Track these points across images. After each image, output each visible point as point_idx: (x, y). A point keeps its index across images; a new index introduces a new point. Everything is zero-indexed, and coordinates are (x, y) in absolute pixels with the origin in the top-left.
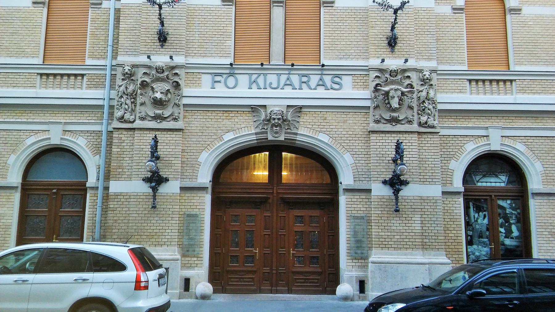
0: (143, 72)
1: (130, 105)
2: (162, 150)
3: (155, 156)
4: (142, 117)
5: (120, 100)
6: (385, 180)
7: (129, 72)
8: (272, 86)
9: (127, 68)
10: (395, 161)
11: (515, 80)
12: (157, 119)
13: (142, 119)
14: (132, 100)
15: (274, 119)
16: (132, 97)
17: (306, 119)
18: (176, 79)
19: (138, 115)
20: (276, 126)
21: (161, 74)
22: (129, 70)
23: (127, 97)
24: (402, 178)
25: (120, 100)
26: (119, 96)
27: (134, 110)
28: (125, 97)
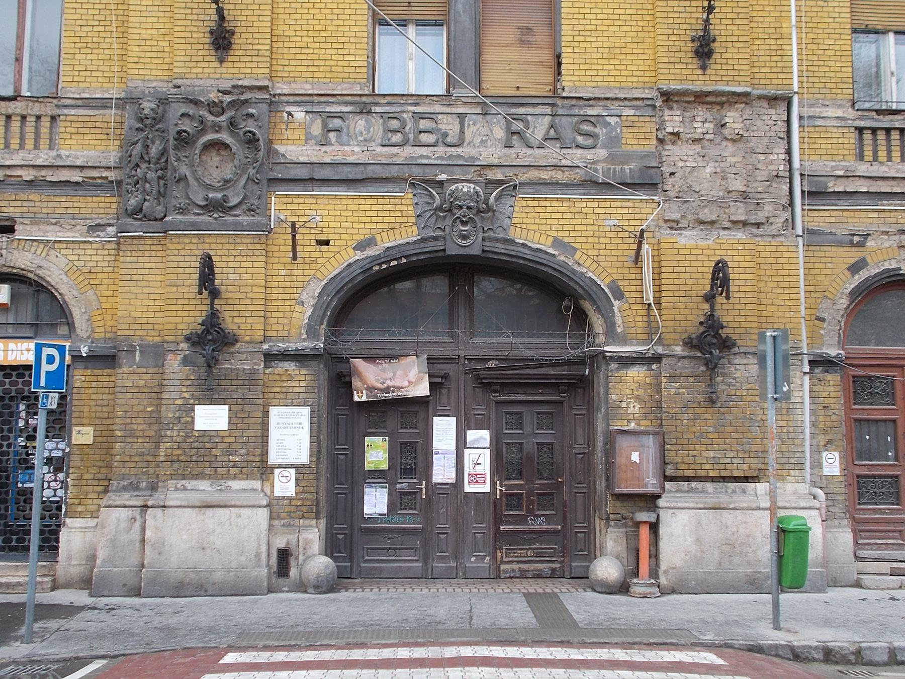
0: (180, 114)
1: (155, 184)
2: (224, 275)
4: (180, 208)
5: (133, 172)
6: (690, 338)
7: (152, 114)
9: (148, 106)
10: (709, 298)
12: (212, 211)
13: (182, 211)
14: (160, 173)
16: (158, 165)
18: (251, 126)
21: (217, 116)
22: (152, 110)
23: (148, 166)
24: (723, 333)
25: (133, 172)
27: (165, 193)
28: (144, 166)
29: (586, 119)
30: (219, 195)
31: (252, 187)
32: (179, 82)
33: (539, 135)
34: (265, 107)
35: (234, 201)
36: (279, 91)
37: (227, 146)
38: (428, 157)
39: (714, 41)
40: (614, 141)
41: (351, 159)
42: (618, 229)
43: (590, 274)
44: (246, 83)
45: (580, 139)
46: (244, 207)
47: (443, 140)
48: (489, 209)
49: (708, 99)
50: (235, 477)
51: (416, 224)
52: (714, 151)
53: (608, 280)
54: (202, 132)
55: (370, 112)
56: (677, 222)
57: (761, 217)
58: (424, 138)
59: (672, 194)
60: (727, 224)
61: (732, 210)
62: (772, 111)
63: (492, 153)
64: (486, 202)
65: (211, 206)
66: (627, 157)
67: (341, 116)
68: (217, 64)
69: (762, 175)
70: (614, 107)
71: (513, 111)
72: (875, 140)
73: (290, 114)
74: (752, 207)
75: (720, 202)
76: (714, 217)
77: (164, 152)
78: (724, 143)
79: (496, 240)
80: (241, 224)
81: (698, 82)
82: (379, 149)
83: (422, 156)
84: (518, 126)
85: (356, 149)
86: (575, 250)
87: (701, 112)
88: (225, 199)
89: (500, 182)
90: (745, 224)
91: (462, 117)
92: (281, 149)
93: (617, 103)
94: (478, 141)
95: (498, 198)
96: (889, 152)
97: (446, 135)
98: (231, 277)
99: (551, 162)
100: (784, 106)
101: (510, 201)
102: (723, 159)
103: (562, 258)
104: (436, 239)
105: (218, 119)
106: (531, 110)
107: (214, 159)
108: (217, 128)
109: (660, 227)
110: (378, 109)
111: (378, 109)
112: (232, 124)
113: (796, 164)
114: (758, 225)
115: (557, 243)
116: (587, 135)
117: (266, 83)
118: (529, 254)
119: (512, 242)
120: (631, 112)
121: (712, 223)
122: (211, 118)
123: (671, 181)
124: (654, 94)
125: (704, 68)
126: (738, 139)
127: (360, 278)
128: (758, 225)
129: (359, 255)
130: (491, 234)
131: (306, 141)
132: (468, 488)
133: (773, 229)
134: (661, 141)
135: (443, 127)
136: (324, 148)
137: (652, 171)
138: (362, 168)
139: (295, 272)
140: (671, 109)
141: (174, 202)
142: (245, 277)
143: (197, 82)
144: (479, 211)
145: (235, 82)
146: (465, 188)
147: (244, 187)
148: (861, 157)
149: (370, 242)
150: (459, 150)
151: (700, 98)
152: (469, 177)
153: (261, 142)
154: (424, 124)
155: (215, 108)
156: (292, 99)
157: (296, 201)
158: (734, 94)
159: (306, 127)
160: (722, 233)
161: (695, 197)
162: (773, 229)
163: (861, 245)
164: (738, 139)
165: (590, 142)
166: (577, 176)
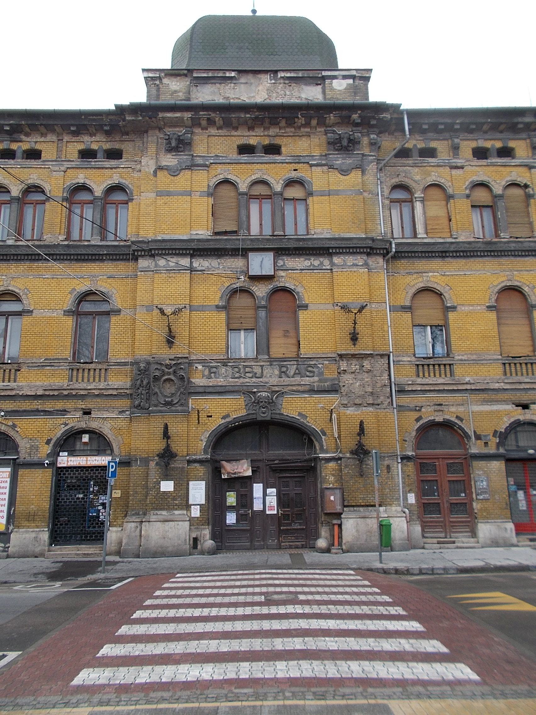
1: (145, 395)
2: (172, 430)
3: (166, 435)
8: (257, 375)
9: (142, 365)
10: (359, 434)
11: (453, 364)
13: (156, 406)
15: (262, 402)
17: (287, 398)
19: (152, 402)
20: (264, 408)
26: (136, 388)
28: (141, 389)
29: (310, 366)
30: (170, 399)
31: (182, 395)
32: (154, 356)
33: (292, 373)
34: (187, 365)
35: (175, 402)
36: (192, 359)
37: (172, 380)
38: (249, 383)
39: (358, 334)
40: (321, 374)
41: (220, 384)
42: (323, 408)
43: (313, 426)
44: (180, 356)
45: (308, 373)
46: (179, 404)
47: (255, 375)
48: (273, 402)
49: (357, 356)
50: (176, 510)
51: (245, 408)
52: (360, 377)
53: (320, 428)
54: (163, 375)
55: (227, 365)
56: (346, 405)
57: (379, 401)
58: (247, 374)
59: (344, 394)
60: (366, 405)
61: (368, 399)
62: (382, 360)
63: (274, 380)
64: (272, 399)
65: (167, 404)
66: (326, 380)
67: (216, 367)
68: (169, 349)
69: (379, 385)
70: (320, 361)
71: (282, 363)
72: (423, 369)
73: (196, 367)
74: (376, 398)
75: (362, 397)
76: (360, 402)
77: (149, 383)
78: (364, 373)
79: (276, 414)
80: (178, 410)
81: (352, 350)
82: (231, 380)
83: (247, 382)
84: (284, 369)
85: (222, 380)
86: (307, 417)
87: (354, 362)
88: (172, 401)
89: (278, 391)
90: (373, 404)
91: (262, 366)
92: (193, 381)
93: (321, 359)
94: (268, 376)
95: (276, 398)
96: (429, 373)
97: (256, 373)
98: (174, 431)
99: (297, 383)
100: (387, 357)
101: (281, 399)
102: (363, 379)
103: (302, 420)
104: (253, 414)
105: (170, 370)
106: (289, 363)
107: (168, 385)
108: (169, 374)
109: (340, 407)
110: (230, 364)
111: (230, 364)
112: (175, 372)
113: (393, 380)
114: (378, 405)
115: (300, 414)
116: (310, 372)
117: (187, 356)
118: (289, 419)
119: (282, 414)
120: (327, 362)
121: (360, 404)
122: (167, 370)
123: (343, 388)
124: (336, 355)
125: (354, 345)
126: (369, 371)
127: (224, 430)
128: (378, 405)
129: (223, 421)
130: (274, 411)
131: (203, 377)
132: (268, 512)
133: (384, 406)
134: (339, 373)
135: (255, 371)
136: (209, 380)
137: (335, 385)
138: (224, 387)
139: (199, 428)
140: (343, 360)
141: (152, 402)
142: (179, 431)
143: (161, 356)
144: (269, 403)
145: (175, 356)
146: (264, 394)
147: (179, 396)
148: (418, 376)
149: (228, 416)
150: (261, 380)
151: (354, 356)
152: (265, 390)
153: (186, 379)
154: (247, 370)
155: (169, 366)
156: (197, 361)
157: (199, 400)
158: (367, 354)
159: (203, 372)
160: (364, 408)
161: (353, 395)
162: (384, 406)
163: (420, 410)
164: (369, 371)
165: (311, 374)
166: (307, 388)
